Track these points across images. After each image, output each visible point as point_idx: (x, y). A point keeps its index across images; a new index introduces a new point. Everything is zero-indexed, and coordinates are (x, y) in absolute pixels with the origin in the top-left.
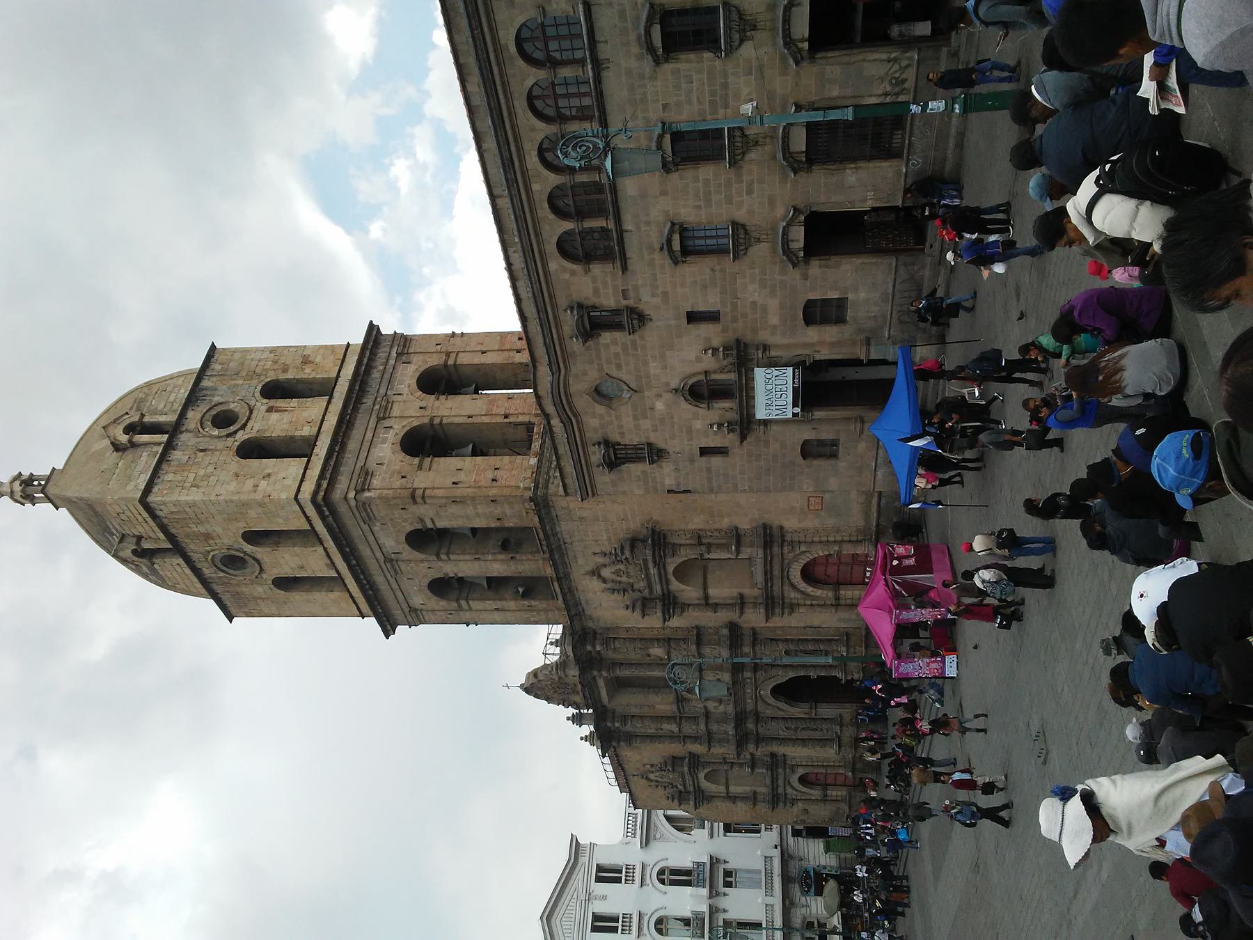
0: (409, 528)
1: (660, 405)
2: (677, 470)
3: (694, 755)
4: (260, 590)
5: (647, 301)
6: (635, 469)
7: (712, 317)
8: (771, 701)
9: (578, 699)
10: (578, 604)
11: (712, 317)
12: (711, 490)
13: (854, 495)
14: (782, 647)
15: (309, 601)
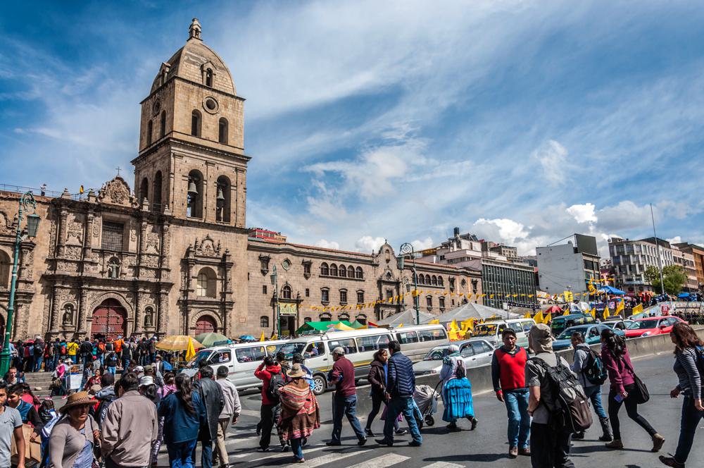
0: (233, 180)
1: (282, 277)
2: (258, 277)
3: (33, 247)
4: (195, 102)
5: (311, 280)
6: (259, 264)
7: (308, 295)
8: (105, 297)
9: (107, 200)
10: (187, 225)
11: (308, 295)
12: (249, 287)
13: (246, 332)
14: (154, 307)
15: (186, 115)
